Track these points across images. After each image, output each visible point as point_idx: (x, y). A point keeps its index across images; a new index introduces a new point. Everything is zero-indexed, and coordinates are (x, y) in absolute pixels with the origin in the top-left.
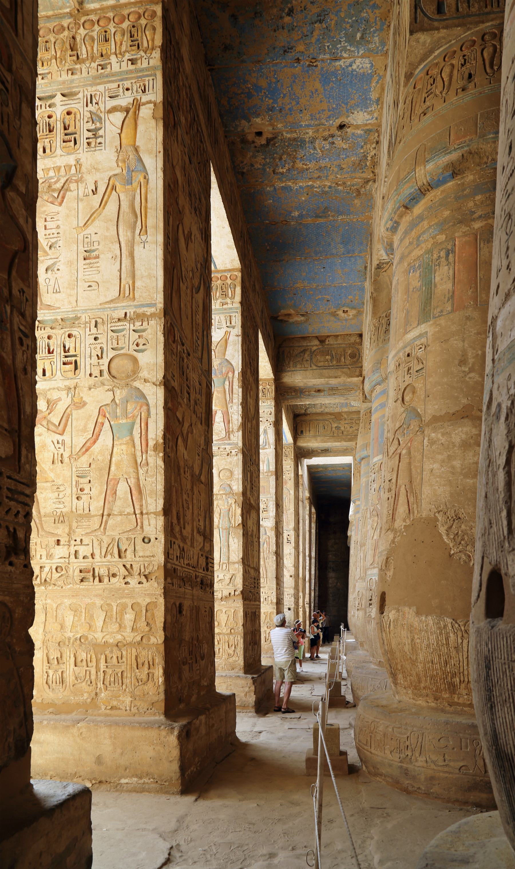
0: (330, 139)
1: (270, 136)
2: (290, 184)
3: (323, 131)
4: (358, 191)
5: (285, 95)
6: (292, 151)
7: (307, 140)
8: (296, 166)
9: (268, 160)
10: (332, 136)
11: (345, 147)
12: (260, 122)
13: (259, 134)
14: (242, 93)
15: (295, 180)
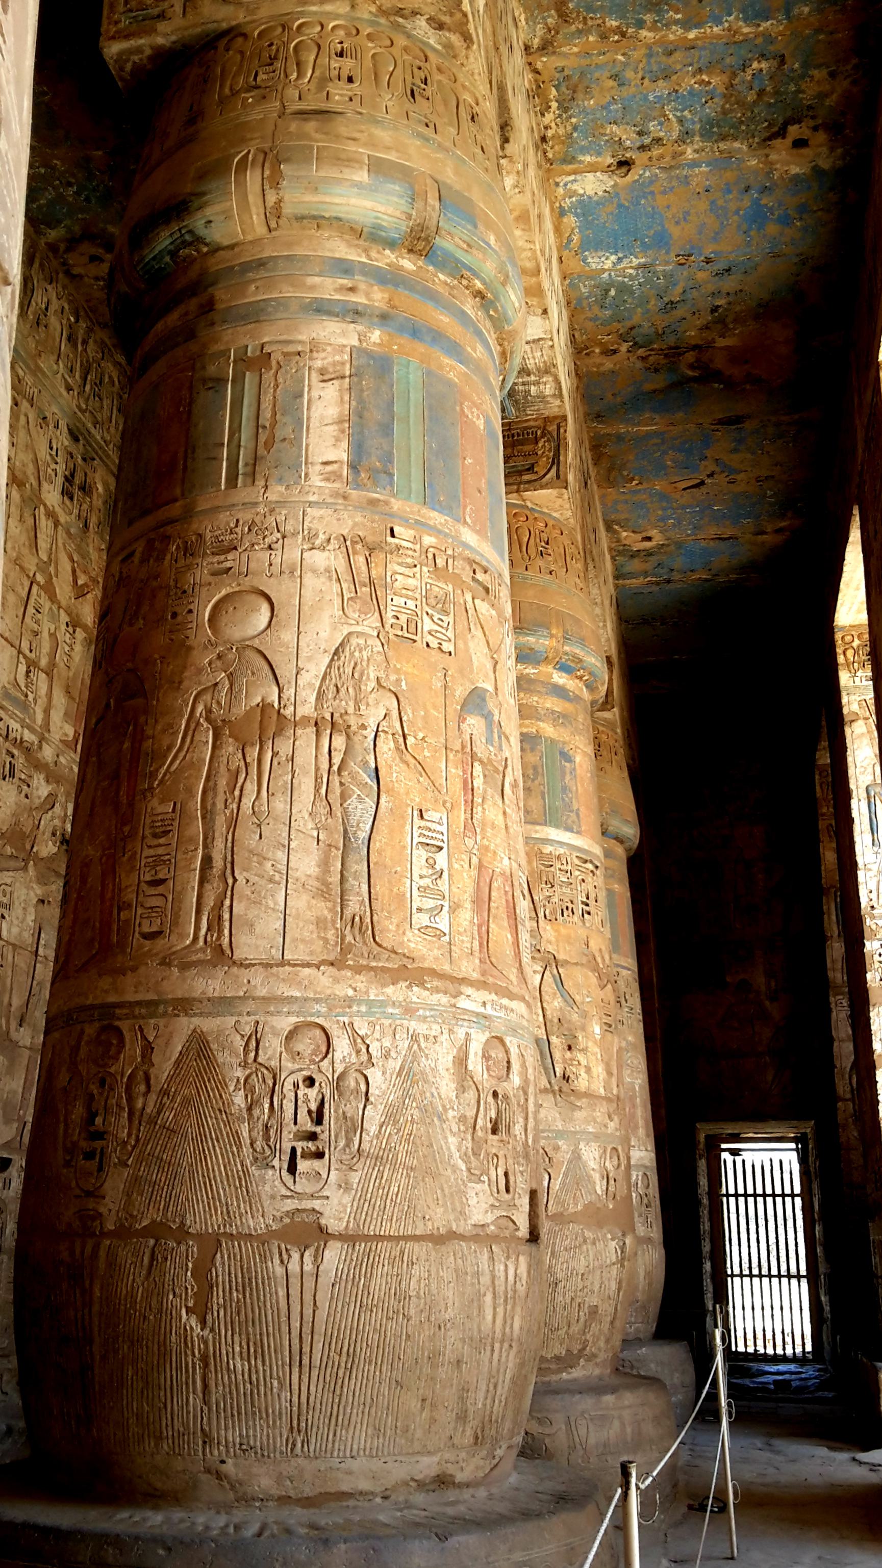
0: (647, 141)
1: (778, 142)
2: (746, 30)
3: (661, 157)
4: (564, 17)
5: (737, 212)
6: (731, 111)
7: (697, 138)
8: (725, 78)
9: (792, 88)
10: (642, 148)
11: (615, 127)
12: (792, 167)
13: (799, 144)
14: (815, 212)
15: (733, 41)
